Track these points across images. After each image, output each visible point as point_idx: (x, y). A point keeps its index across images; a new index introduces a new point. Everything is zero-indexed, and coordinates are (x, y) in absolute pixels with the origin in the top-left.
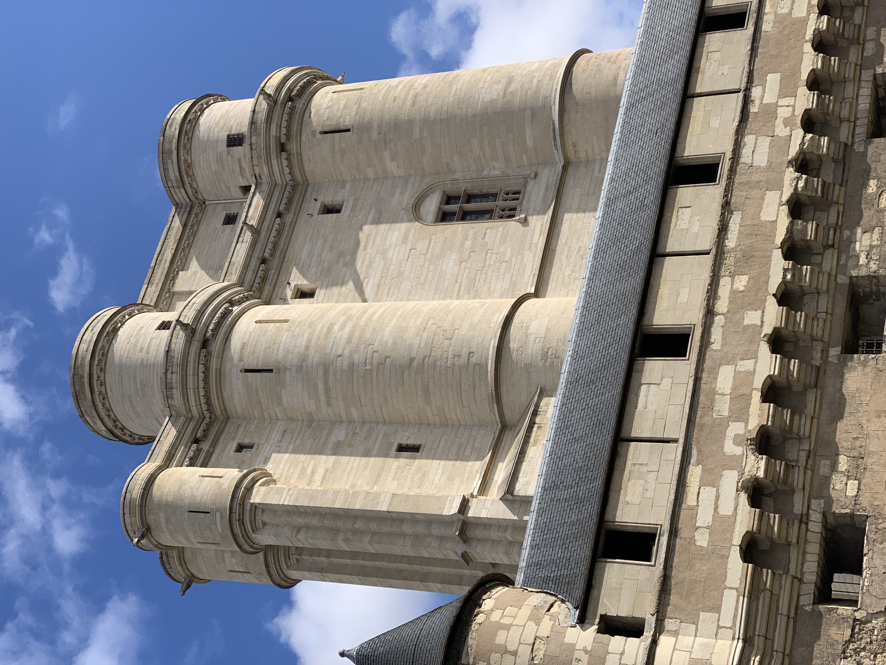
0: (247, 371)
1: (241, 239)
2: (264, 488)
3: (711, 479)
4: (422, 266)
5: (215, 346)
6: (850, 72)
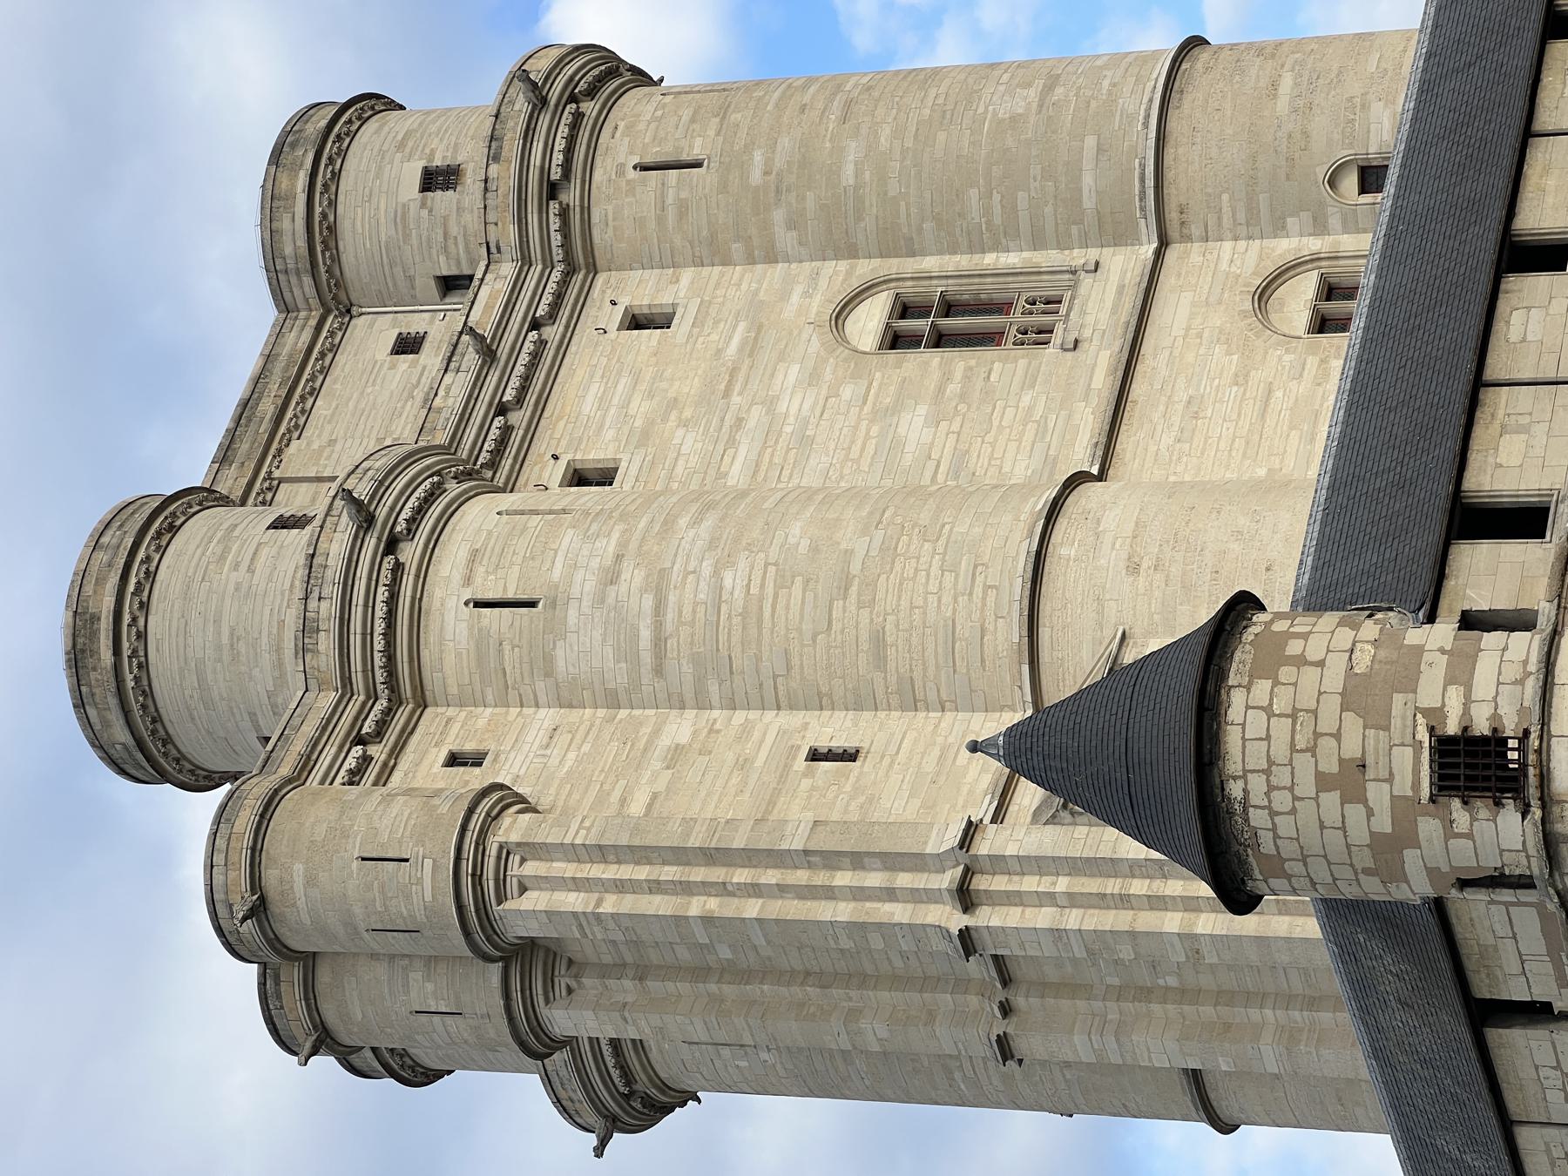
1: (452, 365)
4: (856, 428)
5: (409, 553)
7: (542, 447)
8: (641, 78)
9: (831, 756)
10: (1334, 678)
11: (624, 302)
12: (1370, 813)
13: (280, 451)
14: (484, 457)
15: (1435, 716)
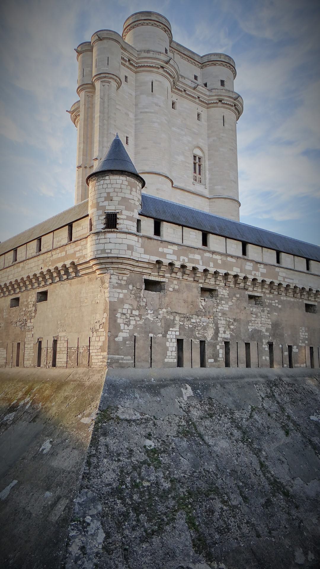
3: (175, 253)
5: (161, 71)
6: (264, 290)
7: (178, 97)
8: (238, 119)
9: (127, 140)
10: (127, 196)
12: (103, 202)
15: (121, 213)
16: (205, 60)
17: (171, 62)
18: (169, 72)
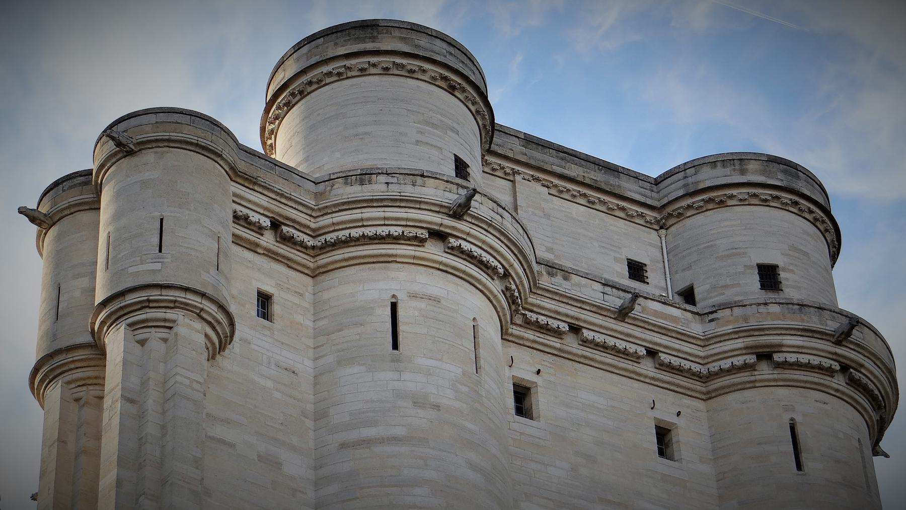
0: (394, 306)
1: (608, 289)
2: (202, 339)
5: (433, 251)
11: (680, 422)
13: (538, 180)
14: (533, 317)
16: (674, 189)
17: (480, 207)
18: (477, 251)
